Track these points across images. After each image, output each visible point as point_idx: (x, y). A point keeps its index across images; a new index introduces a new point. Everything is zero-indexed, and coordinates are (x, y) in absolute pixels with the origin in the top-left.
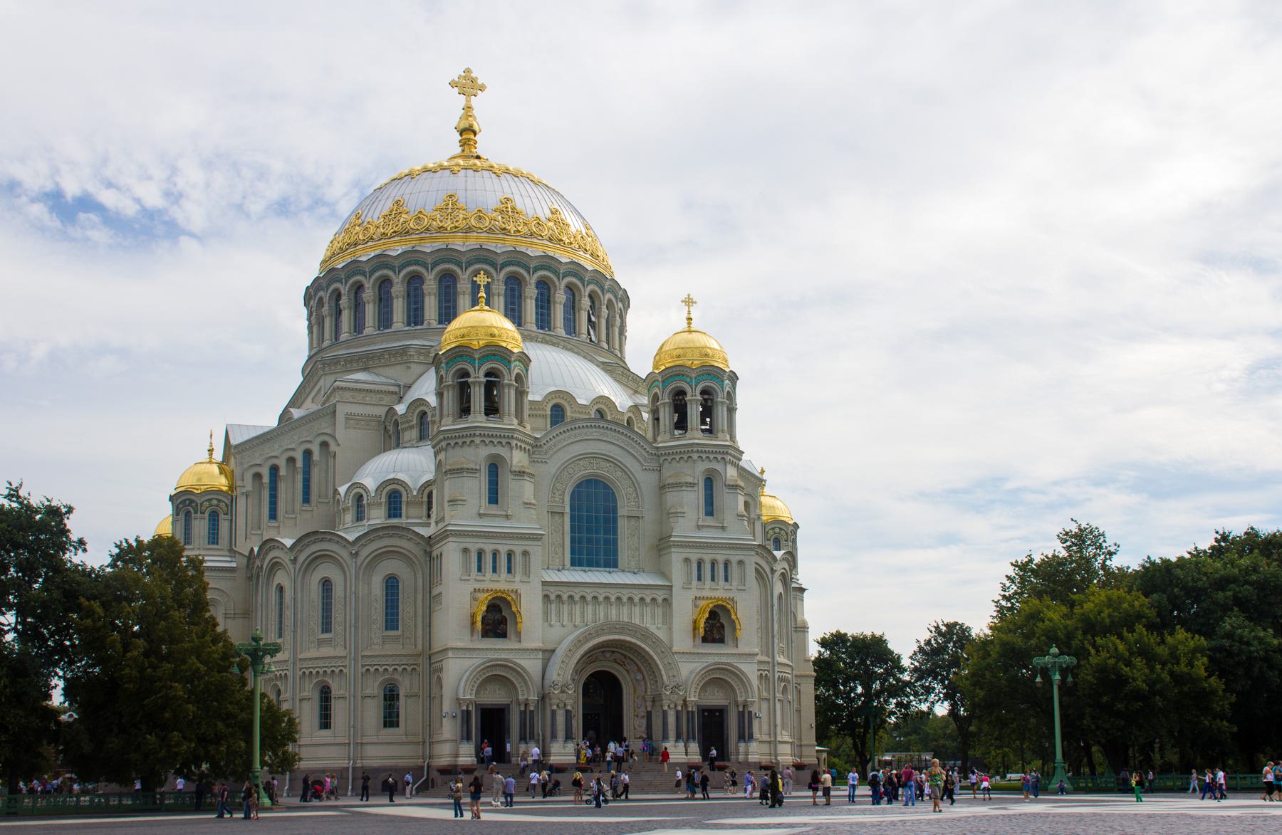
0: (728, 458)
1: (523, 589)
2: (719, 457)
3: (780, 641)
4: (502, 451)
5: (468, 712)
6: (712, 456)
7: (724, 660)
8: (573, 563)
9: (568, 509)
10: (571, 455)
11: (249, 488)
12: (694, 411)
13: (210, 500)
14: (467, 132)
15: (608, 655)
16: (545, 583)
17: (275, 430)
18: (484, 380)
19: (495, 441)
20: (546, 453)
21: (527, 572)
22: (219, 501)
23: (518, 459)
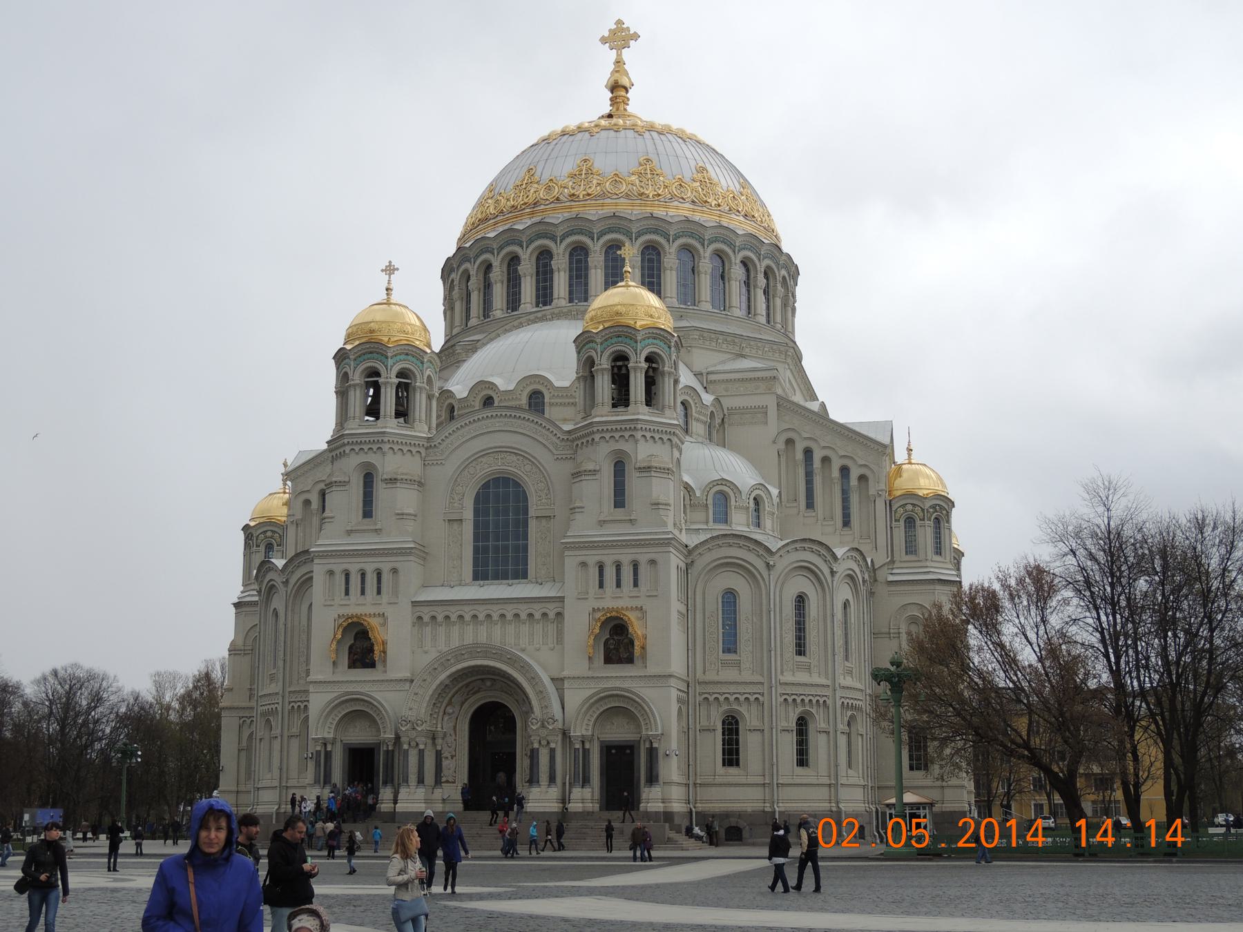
1: (389, 611)
2: (627, 434)
3: (801, 650)
5: (328, 755)
6: (617, 435)
7: (618, 684)
8: (476, 578)
9: (469, 514)
10: (474, 452)
11: (299, 516)
13: (265, 532)
14: (618, 89)
15: (488, 683)
16: (415, 604)
17: (325, 451)
18: (397, 381)
19: (366, 447)
21: (395, 592)
22: (273, 532)
23: (389, 464)
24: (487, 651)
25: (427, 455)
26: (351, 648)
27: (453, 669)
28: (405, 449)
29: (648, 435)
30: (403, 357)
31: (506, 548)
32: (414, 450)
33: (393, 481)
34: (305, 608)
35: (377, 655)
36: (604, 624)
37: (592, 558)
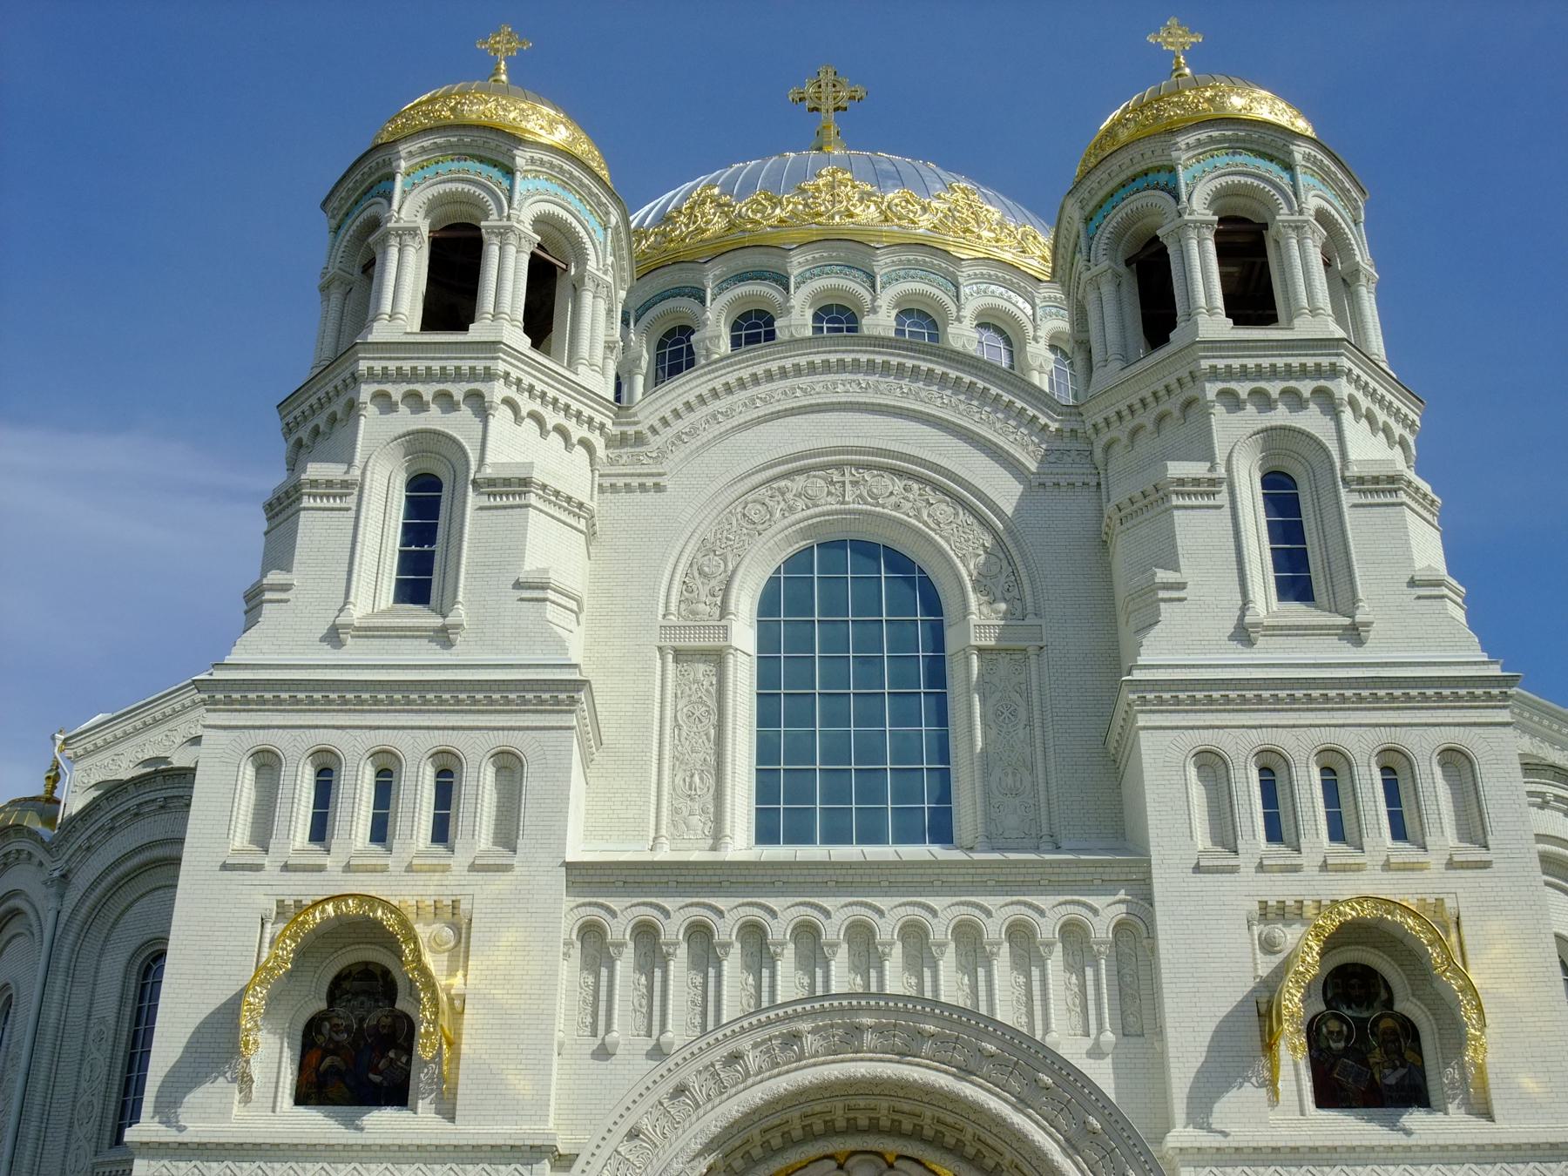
0: (1343, 388)
1: (482, 895)
4: (459, 425)
9: (744, 635)
12: (1202, 275)
20: (662, 455)
23: (507, 444)
24: (908, 1024)
25: (612, 462)
26: (313, 1027)
27: (757, 1095)
28: (552, 418)
29: (1365, 402)
30: (553, 187)
31: (869, 750)
32: (577, 432)
33: (515, 486)
34: (114, 969)
35: (423, 1050)
36: (1331, 944)
37: (1240, 740)
